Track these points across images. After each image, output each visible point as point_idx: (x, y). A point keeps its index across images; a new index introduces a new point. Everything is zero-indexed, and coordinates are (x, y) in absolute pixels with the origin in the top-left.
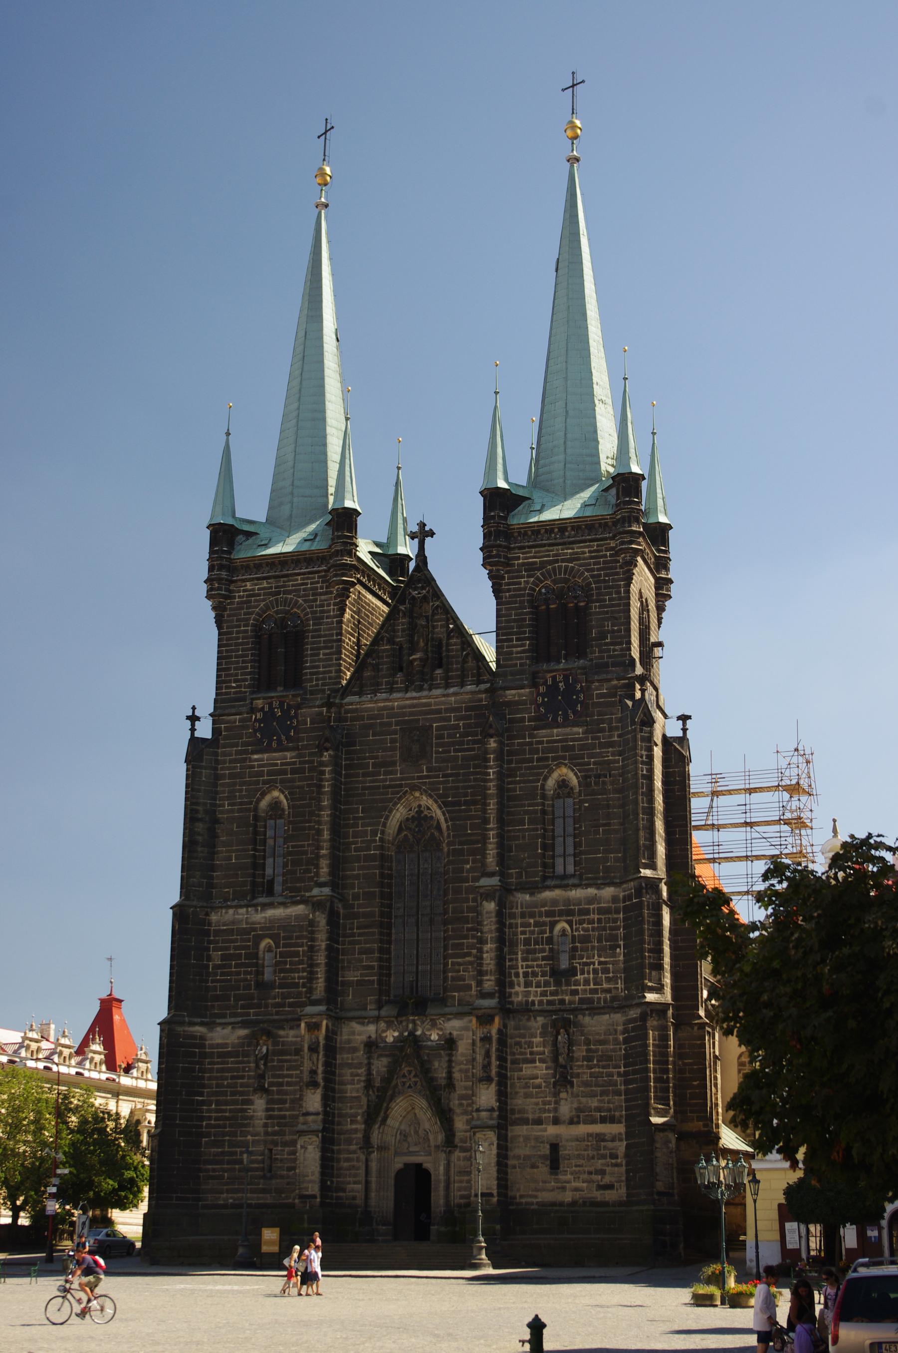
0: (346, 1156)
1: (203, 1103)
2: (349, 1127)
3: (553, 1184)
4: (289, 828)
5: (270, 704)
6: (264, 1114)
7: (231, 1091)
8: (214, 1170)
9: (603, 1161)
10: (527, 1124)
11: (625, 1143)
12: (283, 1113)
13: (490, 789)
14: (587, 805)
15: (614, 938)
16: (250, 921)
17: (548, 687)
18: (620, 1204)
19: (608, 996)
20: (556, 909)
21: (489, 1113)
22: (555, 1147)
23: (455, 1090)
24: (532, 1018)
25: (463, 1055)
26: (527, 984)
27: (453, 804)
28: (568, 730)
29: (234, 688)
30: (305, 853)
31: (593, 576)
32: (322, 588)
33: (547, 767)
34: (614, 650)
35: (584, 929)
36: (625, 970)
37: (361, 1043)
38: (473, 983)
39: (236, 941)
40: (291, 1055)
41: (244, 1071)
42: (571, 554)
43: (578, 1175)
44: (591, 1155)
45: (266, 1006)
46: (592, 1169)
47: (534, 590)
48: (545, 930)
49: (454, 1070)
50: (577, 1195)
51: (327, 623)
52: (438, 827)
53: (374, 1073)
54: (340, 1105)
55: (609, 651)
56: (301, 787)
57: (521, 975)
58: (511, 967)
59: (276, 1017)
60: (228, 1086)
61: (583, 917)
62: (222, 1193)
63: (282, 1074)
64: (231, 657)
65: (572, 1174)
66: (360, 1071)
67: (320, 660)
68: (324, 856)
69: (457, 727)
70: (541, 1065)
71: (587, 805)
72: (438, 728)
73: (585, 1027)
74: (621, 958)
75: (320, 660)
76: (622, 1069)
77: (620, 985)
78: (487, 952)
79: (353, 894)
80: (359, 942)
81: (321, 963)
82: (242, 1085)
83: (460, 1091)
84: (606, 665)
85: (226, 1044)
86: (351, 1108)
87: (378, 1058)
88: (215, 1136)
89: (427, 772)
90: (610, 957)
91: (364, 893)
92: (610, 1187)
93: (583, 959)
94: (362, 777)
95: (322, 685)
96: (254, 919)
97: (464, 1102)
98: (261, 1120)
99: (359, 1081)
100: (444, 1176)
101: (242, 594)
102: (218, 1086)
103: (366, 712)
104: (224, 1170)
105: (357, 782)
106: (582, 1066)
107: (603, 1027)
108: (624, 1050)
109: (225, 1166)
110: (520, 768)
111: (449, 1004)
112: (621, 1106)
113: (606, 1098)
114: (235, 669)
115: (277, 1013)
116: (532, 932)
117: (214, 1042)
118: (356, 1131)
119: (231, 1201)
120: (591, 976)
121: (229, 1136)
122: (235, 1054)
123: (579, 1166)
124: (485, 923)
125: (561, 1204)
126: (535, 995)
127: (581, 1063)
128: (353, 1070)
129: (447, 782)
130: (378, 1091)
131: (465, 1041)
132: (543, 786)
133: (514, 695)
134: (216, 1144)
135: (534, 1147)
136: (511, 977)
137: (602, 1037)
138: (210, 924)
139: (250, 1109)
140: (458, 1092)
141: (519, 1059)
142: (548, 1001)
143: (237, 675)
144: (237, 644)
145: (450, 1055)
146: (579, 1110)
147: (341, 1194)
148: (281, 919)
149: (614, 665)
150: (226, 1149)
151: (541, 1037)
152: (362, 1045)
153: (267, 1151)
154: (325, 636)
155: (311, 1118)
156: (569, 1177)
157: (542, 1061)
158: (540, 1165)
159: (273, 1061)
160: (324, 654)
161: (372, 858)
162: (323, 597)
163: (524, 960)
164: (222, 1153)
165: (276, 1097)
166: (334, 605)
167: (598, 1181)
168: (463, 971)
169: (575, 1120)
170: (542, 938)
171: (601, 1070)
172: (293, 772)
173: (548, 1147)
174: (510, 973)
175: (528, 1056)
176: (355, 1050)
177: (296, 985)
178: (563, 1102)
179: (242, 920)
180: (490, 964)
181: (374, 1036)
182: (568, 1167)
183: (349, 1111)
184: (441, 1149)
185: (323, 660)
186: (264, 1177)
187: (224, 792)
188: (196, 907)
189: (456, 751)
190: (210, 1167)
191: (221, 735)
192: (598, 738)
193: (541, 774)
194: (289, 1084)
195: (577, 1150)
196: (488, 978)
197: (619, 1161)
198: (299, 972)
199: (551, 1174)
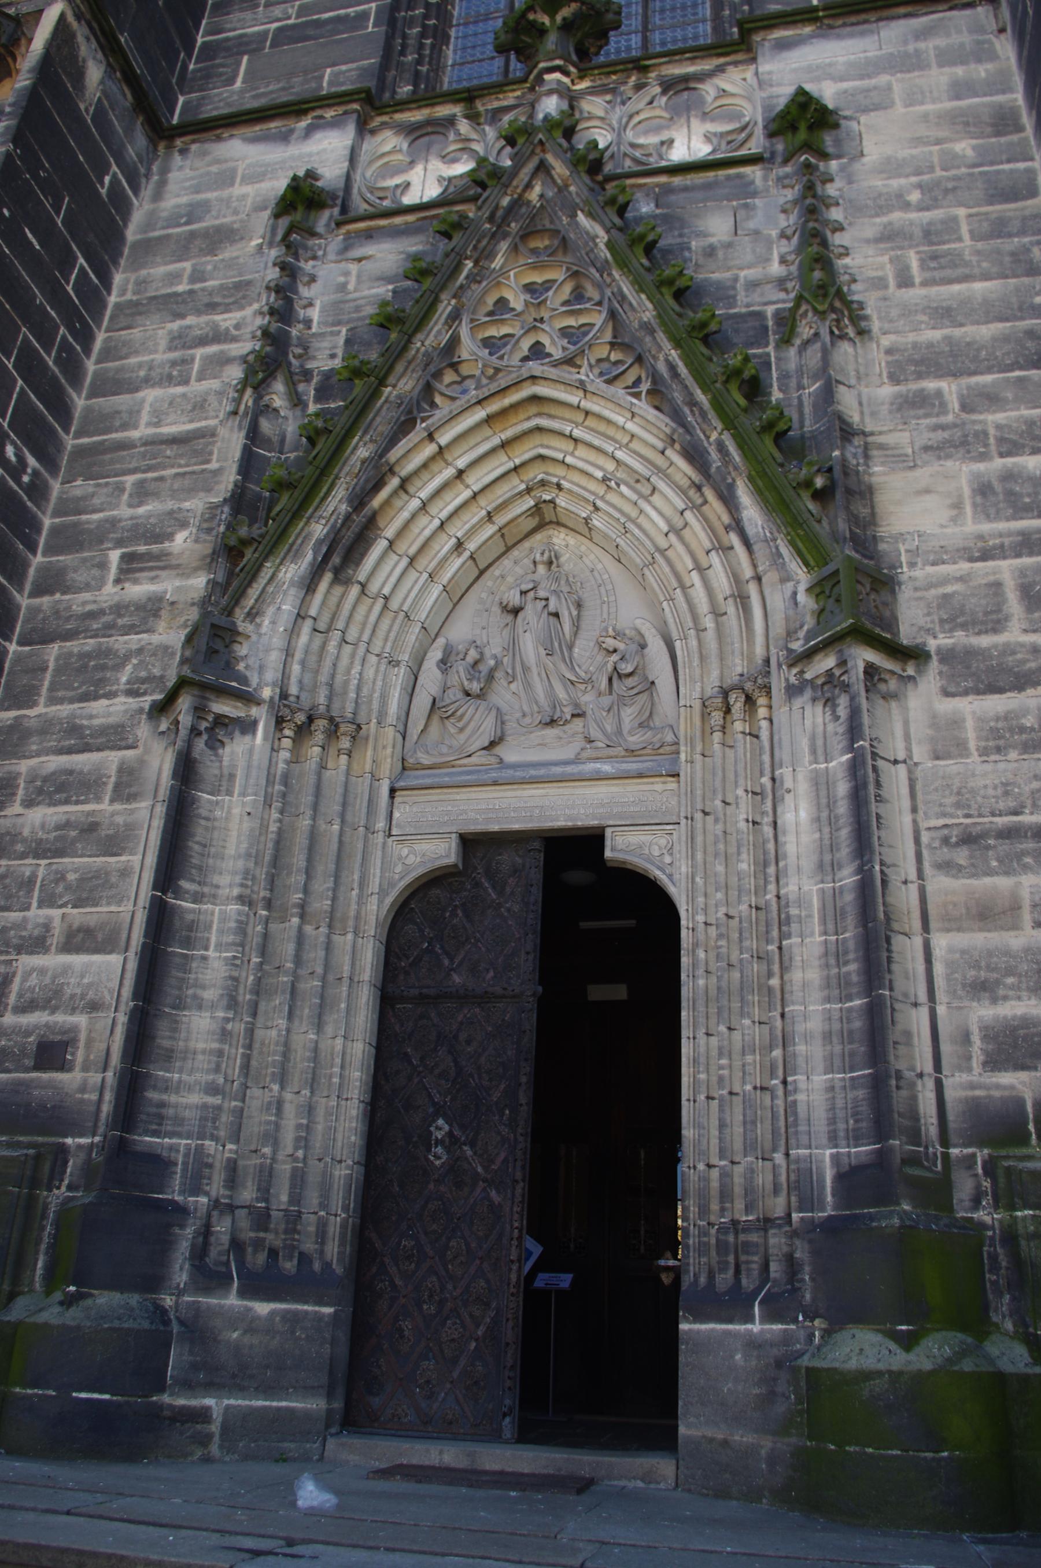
0: (54, 762)
2: (109, 592)
25: (890, 167)
49: (837, 239)
53: (315, 314)
54: (80, 487)
66: (226, 320)
86: (142, 493)
97: (949, 388)
100: (826, 868)
128: (190, 320)
130: (322, 394)
131: (900, 109)
140: (886, 341)
152: (266, 214)
183: (124, 511)
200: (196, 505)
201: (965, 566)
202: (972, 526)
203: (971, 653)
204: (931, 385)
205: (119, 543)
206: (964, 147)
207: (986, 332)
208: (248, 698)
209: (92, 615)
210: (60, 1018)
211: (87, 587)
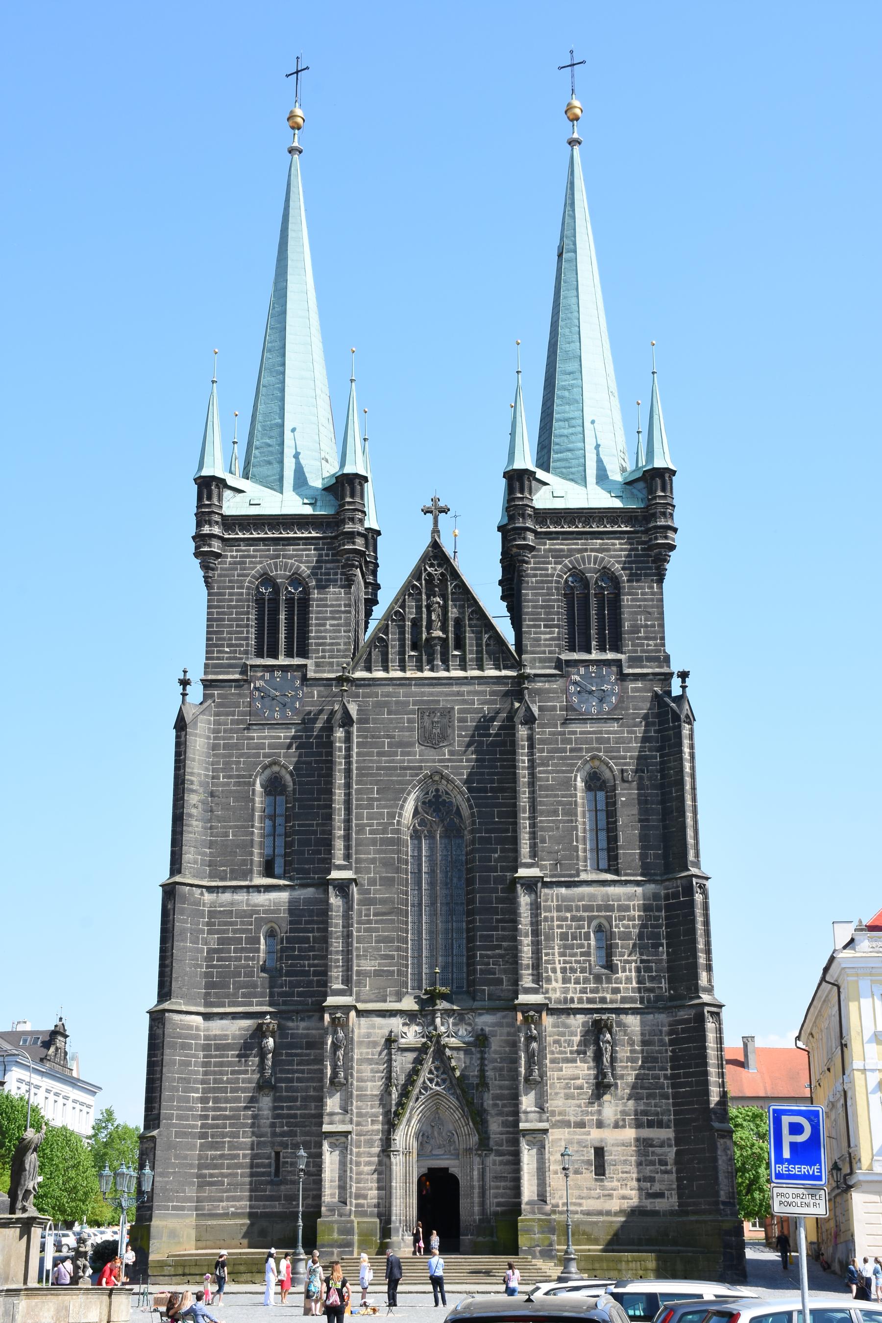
0: (367, 1159)
2: (370, 1127)
3: (598, 1191)
4: (294, 806)
7: (231, 1087)
8: (211, 1175)
9: (652, 1168)
10: (570, 1127)
11: (675, 1149)
14: (624, 799)
15: (657, 936)
16: (252, 902)
18: (672, 1213)
19: (652, 995)
20: (595, 903)
22: (600, 1152)
23: (489, 1090)
25: (496, 1052)
26: (565, 980)
27: (479, 790)
29: (227, 653)
30: (315, 833)
32: (327, 555)
33: (580, 758)
34: (648, 645)
35: (623, 926)
36: (670, 969)
40: (301, 1048)
42: (601, 544)
43: (625, 1182)
48: (584, 925)
49: (486, 1068)
52: (458, 812)
55: (642, 645)
56: (310, 763)
57: (559, 971)
58: (547, 962)
60: (228, 1081)
61: (623, 914)
62: (222, 1201)
63: (292, 1069)
64: (224, 620)
67: (326, 631)
70: (583, 1064)
71: (624, 799)
72: (461, 711)
73: (628, 1027)
74: (665, 957)
75: (326, 631)
76: (669, 1072)
77: (664, 985)
79: (369, 879)
80: (376, 930)
83: (494, 1091)
84: (640, 659)
85: (226, 1035)
88: (213, 1136)
89: (449, 755)
91: (381, 878)
92: (660, 1195)
93: (623, 956)
94: (377, 756)
95: (329, 658)
96: (256, 901)
98: (268, 1119)
100: (479, 1181)
101: (234, 553)
102: (215, 1081)
104: (223, 1175)
105: (371, 761)
106: (627, 1067)
108: (672, 1051)
110: (553, 758)
111: (478, 998)
112: (670, 1111)
114: (228, 633)
116: (570, 927)
119: (233, 1209)
120: (633, 974)
121: (230, 1137)
123: (626, 1172)
126: (574, 992)
127: (625, 1064)
128: (373, 1066)
136: (547, 972)
141: (559, 1058)
142: (587, 998)
143: (230, 639)
144: (229, 607)
145: (482, 1053)
147: (361, 1201)
149: (650, 659)
153: (273, 1154)
154: (332, 606)
156: (615, 1184)
158: (584, 1171)
159: (281, 1054)
160: (331, 625)
161: (391, 842)
162: (329, 565)
164: (222, 1156)
165: (284, 1094)
166: (341, 575)
167: (647, 1189)
168: (493, 965)
169: (621, 1123)
170: (580, 933)
171: (647, 1072)
173: (593, 1151)
174: (547, 968)
175: (568, 1055)
176: (375, 1044)
177: (306, 973)
178: (606, 1104)
179: (242, 902)
182: (614, 1174)
184: (474, 1152)
185: (330, 631)
186: (271, 1183)
190: (207, 1171)
193: (574, 765)
194: (299, 1080)
195: (623, 1156)
197: (669, 1167)
198: (309, 960)
199: (596, 1180)
201: (499, 1136)
202: (501, 1129)
203: (499, 1150)
204: (498, 1102)
205: (370, 1117)
206: (507, 1049)
207: (506, 1092)
209: (368, 1131)
211: (365, 1126)
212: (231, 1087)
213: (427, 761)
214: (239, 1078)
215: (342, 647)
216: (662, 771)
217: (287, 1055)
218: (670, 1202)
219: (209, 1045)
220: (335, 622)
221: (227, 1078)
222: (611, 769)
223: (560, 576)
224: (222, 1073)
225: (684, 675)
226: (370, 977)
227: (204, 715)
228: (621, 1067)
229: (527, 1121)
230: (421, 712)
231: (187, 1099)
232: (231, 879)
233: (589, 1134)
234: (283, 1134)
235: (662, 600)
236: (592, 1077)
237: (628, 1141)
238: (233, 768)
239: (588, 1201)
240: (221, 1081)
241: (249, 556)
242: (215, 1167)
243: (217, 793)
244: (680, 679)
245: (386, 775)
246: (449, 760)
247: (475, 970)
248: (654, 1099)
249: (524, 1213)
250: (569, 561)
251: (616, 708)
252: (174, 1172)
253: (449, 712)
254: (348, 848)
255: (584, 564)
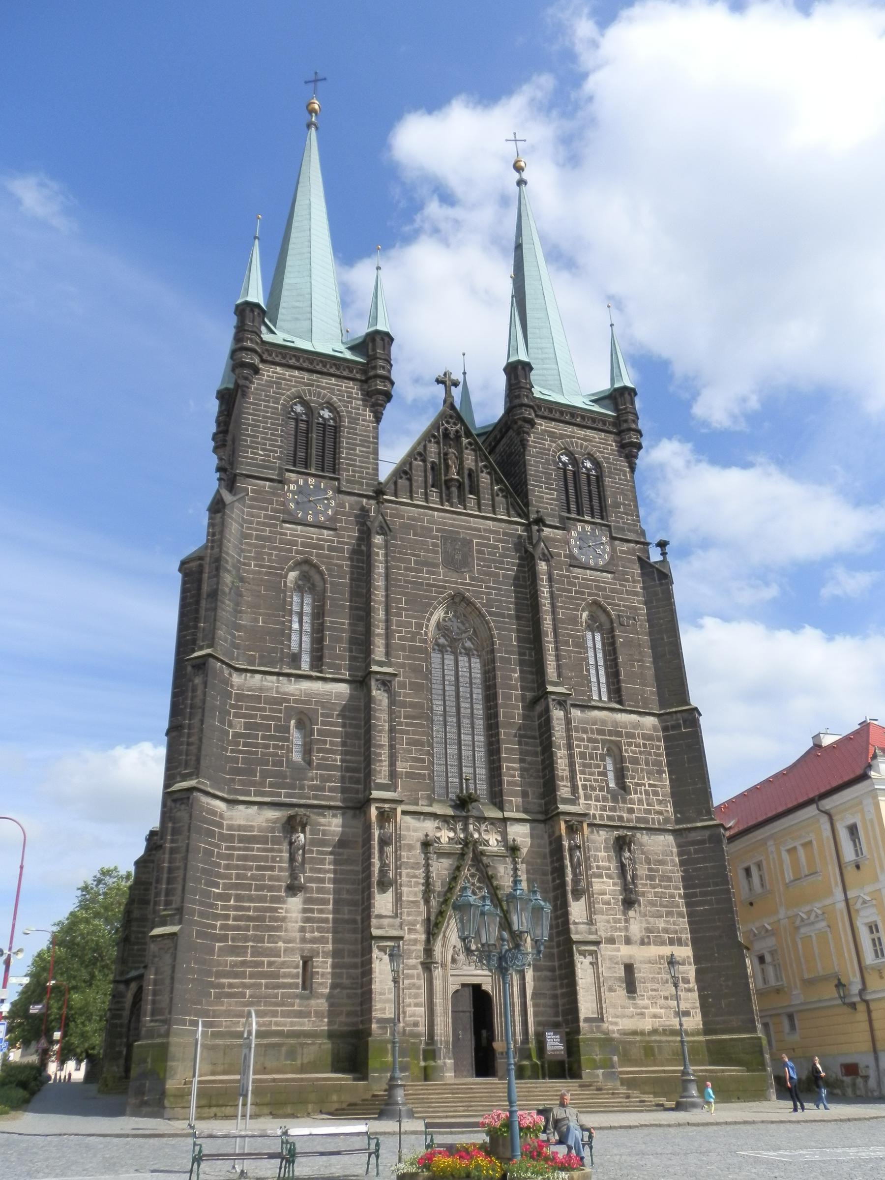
1: (220, 897)
3: (632, 1009)
5: (306, 482)
6: (300, 915)
8: (231, 986)
12: (324, 916)
13: (545, 606)
15: (658, 763)
16: (282, 690)
17: (579, 533)
19: (661, 817)
21: (588, 926)
22: (629, 969)
24: (595, 831)
28: (598, 573)
29: (261, 455)
31: (603, 457)
33: (584, 600)
34: (627, 519)
36: (673, 795)
37: (417, 841)
38: (529, 790)
39: (264, 710)
41: (273, 859)
42: (584, 435)
44: (664, 979)
45: (302, 788)
46: (667, 994)
47: (556, 453)
50: (657, 1023)
51: (363, 425)
55: (623, 518)
56: (341, 566)
59: (315, 802)
60: (253, 878)
65: (649, 999)
66: (417, 872)
67: (356, 455)
68: (379, 635)
69: (497, 547)
72: (478, 544)
74: (668, 783)
77: (670, 808)
78: (561, 758)
81: (384, 745)
82: (271, 878)
85: (252, 826)
87: (438, 859)
88: (233, 940)
90: (658, 781)
91: (410, 683)
92: (687, 1014)
93: (634, 779)
96: (287, 690)
98: (297, 922)
99: (417, 883)
101: (271, 374)
102: (238, 877)
103: (407, 513)
104: (244, 986)
106: (646, 884)
107: (660, 848)
109: (247, 981)
110: (561, 596)
113: (672, 920)
114: (263, 438)
115: (315, 797)
116: (587, 747)
117: (234, 823)
118: (415, 942)
120: (644, 796)
121: (253, 941)
122: (264, 840)
123: (655, 990)
124: (557, 729)
125: (642, 1033)
128: (409, 870)
129: (491, 594)
130: (439, 896)
132: (581, 615)
133: (550, 532)
134: (234, 951)
135: (610, 968)
137: (661, 858)
138: (232, 686)
139: (282, 908)
142: (607, 815)
144: (264, 417)
146: (648, 930)
148: (319, 694)
149: (629, 531)
150: (249, 958)
151: (605, 852)
153: (301, 962)
155: (386, 921)
157: (609, 876)
159: (312, 852)
160: (360, 451)
163: (583, 773)
164: (243, 964)
169: (646, 940)
170: (596, 753)
171: (664, 891)
172: (331, 549)
175: (595, 870)
176: (410, 847)
179: (272, 688)
180: (565, 770)
181: (431, 834)
182: (644, 992)
186: (301, 997)
187: (250, 551)
188: (223, 662)
189: (496, 568)
190: (225, 981)
191: (247, 495)
192: (625, 586)
195: (651, 973)
196: (564, 783)
197: (691, 985)
199: (629, 998)
200: (420, 919)
205: (407, 925)
206: (539, 861)
208: (437, 963)
210: (416, 1019)
212: (255, 884)
213: (451, 582)
214: (265, 875)
215: (370, 471)
216: (649, 621)
217: (319, 852)
218: (694, 1022)
219: (233, 836)
220: (365, 449)
221: (252, 874)
222: (608, 614)
223: (553, 451)
224: (246, 868)
225: (662, 544)
226: (402, 778)
227: (239, 503)
228: (642, 884)
229: (577, 933)
230: (445, 539)
231: (208, 894)
232: (260, 665)
233: (618, 950)
234: (314, 941)
235: (634, 487)
236: (618, 893)
237: (654, 958)
238: (265, 558)
239: (624, 1019)
240: (245, 877)
241: (285, 379)
242: (236, 975)
243: (248, 580)
244: (659, 549)
245: (412, 589)
246: (470, 585)
247: (500, 783)
248: (672, 917)
249: (582, 1032)
250: (562, 442)
251: (608, 563)
252: (194, 979)
253: (469, 543)
254: (388, 646)
255: (573, 447)
